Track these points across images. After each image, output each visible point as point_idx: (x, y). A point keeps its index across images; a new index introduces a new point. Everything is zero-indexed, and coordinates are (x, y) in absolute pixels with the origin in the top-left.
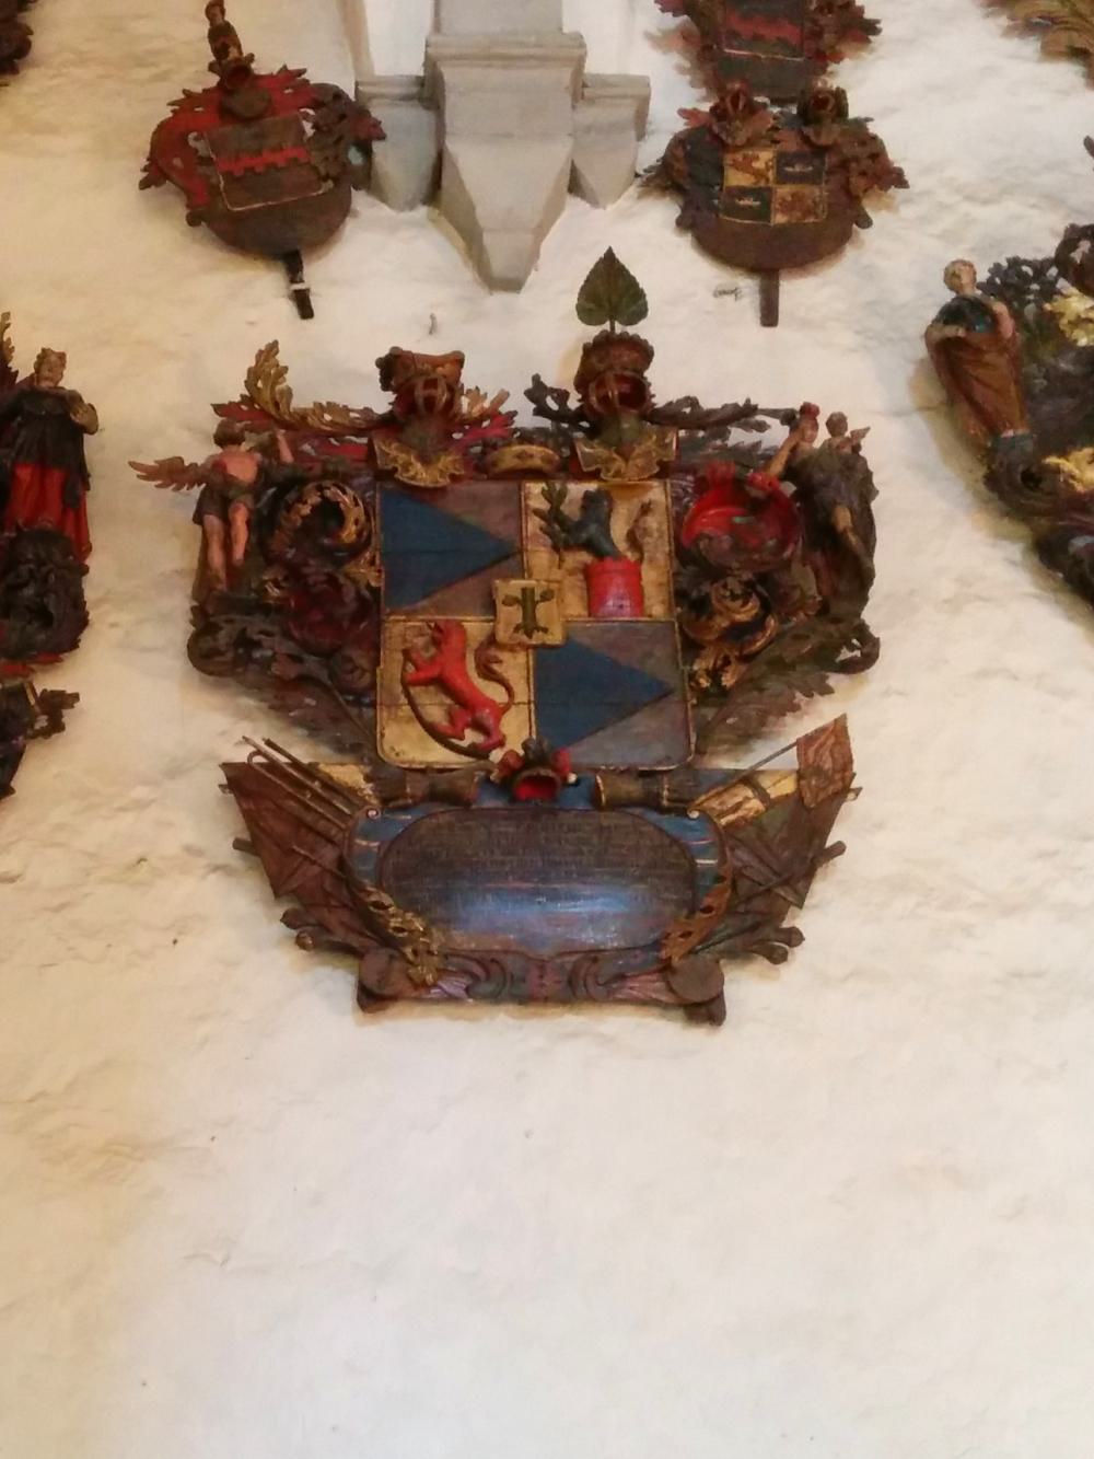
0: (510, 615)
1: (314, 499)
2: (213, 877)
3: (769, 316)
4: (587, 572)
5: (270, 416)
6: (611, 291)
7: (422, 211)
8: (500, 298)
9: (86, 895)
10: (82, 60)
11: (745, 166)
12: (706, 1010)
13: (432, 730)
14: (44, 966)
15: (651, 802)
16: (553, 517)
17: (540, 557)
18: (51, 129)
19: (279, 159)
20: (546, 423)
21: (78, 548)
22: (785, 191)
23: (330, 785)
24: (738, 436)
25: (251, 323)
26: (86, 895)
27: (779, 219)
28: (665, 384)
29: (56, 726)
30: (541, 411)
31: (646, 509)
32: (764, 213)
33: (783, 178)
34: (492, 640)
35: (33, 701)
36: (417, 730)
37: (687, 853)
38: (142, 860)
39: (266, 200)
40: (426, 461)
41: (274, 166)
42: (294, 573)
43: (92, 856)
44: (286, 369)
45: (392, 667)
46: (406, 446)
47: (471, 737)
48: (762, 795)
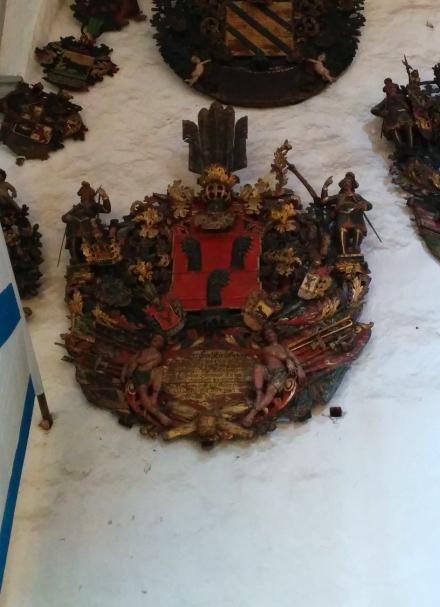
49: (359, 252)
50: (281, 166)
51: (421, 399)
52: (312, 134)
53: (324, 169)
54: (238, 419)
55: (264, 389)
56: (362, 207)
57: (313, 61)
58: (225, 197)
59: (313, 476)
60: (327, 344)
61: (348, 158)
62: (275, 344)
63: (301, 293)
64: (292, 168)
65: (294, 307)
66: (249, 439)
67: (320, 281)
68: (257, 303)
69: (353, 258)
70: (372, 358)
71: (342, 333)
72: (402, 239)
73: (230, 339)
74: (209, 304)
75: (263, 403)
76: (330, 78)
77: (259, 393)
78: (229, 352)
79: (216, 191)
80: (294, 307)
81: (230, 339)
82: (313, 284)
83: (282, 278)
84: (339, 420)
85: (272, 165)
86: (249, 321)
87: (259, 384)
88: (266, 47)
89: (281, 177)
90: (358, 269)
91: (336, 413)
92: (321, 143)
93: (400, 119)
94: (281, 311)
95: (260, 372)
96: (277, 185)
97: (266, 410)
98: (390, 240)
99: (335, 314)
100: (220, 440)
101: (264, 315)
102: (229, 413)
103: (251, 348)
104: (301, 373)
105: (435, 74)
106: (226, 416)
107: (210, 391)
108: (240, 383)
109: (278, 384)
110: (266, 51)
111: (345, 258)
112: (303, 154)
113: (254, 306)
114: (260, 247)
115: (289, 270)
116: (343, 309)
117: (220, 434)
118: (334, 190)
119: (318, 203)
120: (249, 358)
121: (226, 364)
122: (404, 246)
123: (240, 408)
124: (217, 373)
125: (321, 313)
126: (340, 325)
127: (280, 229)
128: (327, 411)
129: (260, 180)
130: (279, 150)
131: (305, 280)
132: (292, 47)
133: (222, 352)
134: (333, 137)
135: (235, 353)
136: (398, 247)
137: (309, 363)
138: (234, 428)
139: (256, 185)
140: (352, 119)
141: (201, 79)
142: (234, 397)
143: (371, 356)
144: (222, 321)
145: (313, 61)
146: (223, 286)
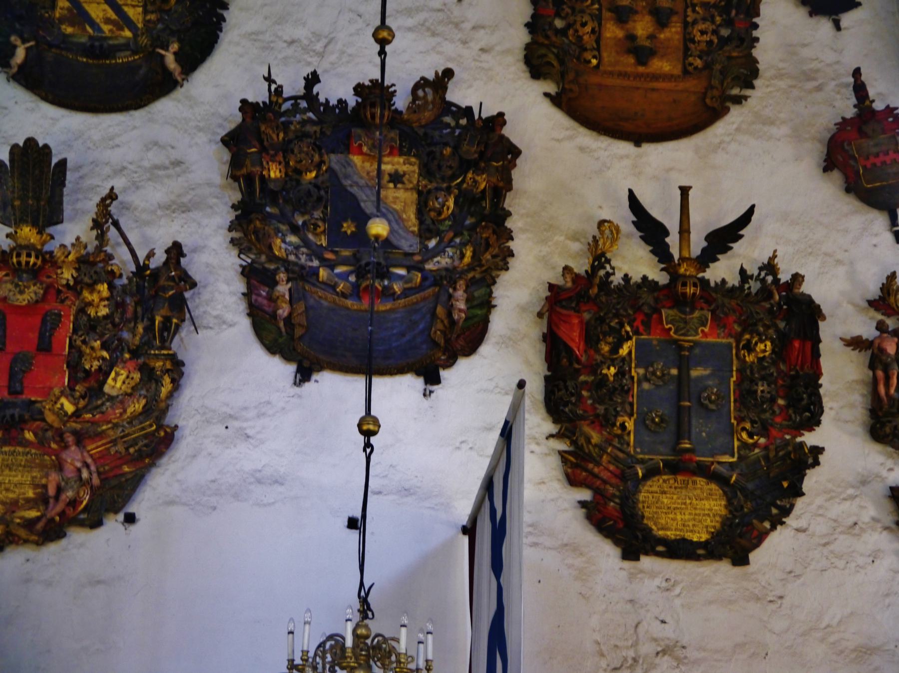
2: (885, 533)
5: (893, 309)
10: (780, 76)
18: (771, 122)
19: (888, 159)
25: (875, 246)
29: (816, 463)
35: (807, 451)
38: (856, 524)
39: (881, 182)
41: (884, 163)
43: (835, 521)
49: (170, 349)
50: (104, 218)
51: (214, 508)
52: (155, 157)
53: (159, 213)
54: (29, 524)
55: (57, 498)
56: (194, 265)
57: (163, 52)
58: (35, 264)
59: (99, 582)
60: (127, 449)
61: (189, 197)
62: (73, 448)
63: (106, 389)
64: (116, 224)
65: (99, 402)
66: (39, 544)
67: (128, 377)
68: (58, 398)
69: (164, 355)
70: (174, 462)
71: (146, 436)
72: (229, 317)
73: (29, 436)
74: (10, 393)
75: (54, 512)
76: (179, 79)
77: (52, 501)
78: (28, 450)
79: (24, 259)
80: (99, 402)
81: (29, 436)
82: (121, 378)
83: (88, 373)
84: (133, 528)
85: (93, 220)
86: (50, 418)
87: (52, 491)
88: (107, 21)
89: (102, 237)
90: (168, 365)
91: (130, 519)
92: (161, 173)
93: (248, 162)
94: (85, 407)
95: (54, 478)
96: (97, 247)
97: (57, 518)
98: (216, 317)
99: (140, 414)
100: (11, 543)
101: (66, 413)
102: (21, 518)
103: (50, 447)
104: (96, 481)
105: (305, 88)
106: (18, 521)
107: (4, 492)
108: (35, 486)
109: (70, 494)
110: (106, 28)
111: (155, 355)
112: (138, 188)
113: (56, 403)
114: (71, 326)
115: (96, 364)
116: (147, 411)
117: (11, 538)
118: (160, 258)
119: (141, 269)
120: (46, 457)
121: (23, 463)
122: (231, 326)
123: (33, 514)
124: (14, 473)
125: (125, 411)
126: (143, 429)
127: (92, 312)
128: (121, 517)
129: (78, 239)
130: (103, 200)
131: (113, 374)
132: (140, 25)
133: (20, 449)
134: (178, 163)
135: (33, 451)
136: (224, 326)
137: (107, 468)
138: (22, 533)
139: (73, 245)
140: (202, 138)
141: (21, 67)
142: (28, 500)
143: (173, 459)
144: (21, 417)
145: (163, 52)
146: (24, 372)
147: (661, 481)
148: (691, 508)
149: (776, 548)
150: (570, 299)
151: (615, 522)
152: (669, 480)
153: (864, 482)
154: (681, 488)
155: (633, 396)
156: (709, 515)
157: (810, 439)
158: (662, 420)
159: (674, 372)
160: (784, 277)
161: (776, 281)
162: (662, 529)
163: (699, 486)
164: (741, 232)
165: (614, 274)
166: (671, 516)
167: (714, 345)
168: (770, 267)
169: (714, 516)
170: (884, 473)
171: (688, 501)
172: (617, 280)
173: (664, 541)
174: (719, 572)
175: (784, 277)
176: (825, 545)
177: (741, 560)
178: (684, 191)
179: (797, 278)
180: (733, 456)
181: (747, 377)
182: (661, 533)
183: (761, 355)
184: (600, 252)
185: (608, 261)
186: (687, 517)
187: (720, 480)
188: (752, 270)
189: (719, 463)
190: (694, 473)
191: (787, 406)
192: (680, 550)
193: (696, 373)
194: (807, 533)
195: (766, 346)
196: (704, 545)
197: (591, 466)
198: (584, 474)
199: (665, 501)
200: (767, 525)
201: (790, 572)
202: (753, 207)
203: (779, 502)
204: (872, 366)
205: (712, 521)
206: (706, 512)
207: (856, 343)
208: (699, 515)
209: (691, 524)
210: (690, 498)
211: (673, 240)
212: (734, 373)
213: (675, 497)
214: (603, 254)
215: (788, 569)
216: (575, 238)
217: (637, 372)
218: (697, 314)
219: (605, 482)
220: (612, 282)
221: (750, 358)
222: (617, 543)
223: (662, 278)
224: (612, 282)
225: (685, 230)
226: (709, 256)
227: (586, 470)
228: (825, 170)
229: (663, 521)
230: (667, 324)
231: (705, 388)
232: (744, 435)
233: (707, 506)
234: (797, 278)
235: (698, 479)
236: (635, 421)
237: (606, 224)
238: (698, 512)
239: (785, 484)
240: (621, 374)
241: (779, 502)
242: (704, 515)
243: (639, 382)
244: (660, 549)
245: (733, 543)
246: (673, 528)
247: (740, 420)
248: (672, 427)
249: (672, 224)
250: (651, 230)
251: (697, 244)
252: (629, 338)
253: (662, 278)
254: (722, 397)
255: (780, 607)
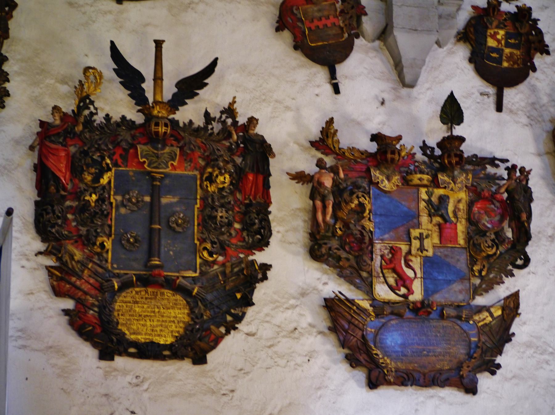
0: (416, 244)
1: (356, 202)
2: (319, 337)
3: (499, 108)
4: (439, 225)
5: (331, 149)
6: (452, 112)
7: (377, 43)
8: (405, 91)
9: (279, 342)
11: (494, 36)
12: (471, 389)
13: (390, 287)
14: (267, 368)
15: (459, 318)
16: (429, 202)
17: (424, 219)
20: (426, 159)
21: (268, 202)
22: (507, 51)
23: (359, 307)
24: (490, 170)
25: (317, 95)
26: (279, 342)
27: (505, 64)
28: (467, 149)
29: (265, 278)
30: (425, 154)
31: (459, 201)
32: (499, 61)
33: (508, 45)
34: (409, 253)
35: (257, 268)
36: (386, 287)
37: (468, 336)
38: (296, 329)
39: (323, 42)
40: (389, 179)
42: (346, 225)
43: (279, 326)
44: (337, 130)
45: (377, 261)
46: (382, 173)
47: (403, 291)
48: (491, 315)
147: (134, 292)
148: (159, 317)
149: (230, 350)
150: (58, 134)
151: (93, 327)
152: (140, 291)
153: (303, 294)
154: (151, 299)
155: (111, 220)
156: (174, 322)
157: (260, 257)
158: (136, 241)
159: (147, 199)
160: (242, 120)
161: (235, 123)
162: (134, 333)
163: (166, 297)
164: (206, 81)
165: (96, 114)
166: (142, 322)
167: (181, 176)
168: (230, 111)
169: (178, 322)
170: (320, 287)
171: (157, 310)
172: (99, 118)
173: (135, 344)
174: (183, 369)
175: (242, 120)
176: (270, 347)
177: (200, 359)
178: (159, 44)
179: (252, 121)
180: (196, 272)
181: (209, 205)
182: (133, 337)
183: (221, 186)
184: (85, 94)
185: (92, 103)
186: (155, 323)
187: (185, 292)
188: (215, 113)
189: (184, 277)
190: (162, 286)
191: (243, 229)
192: (149, 351)
193: (164, 200)
194: (256, 336)
195: (225, 178)
196: (169, 347)
197: (74, 279)
198: (68, 286)
199: (137, 309)
200: (223, 330)
201: (241, 370)
202: (217, 59)
203: (233, 311)
204: (312, 197)
205: (176, 327)
206: (172, 319)
207: (300, 177)
208: (166, 321)
209: (158, 329)
210: (158, 308)
211: (148, 86)
212: (198, 201)
213: (145, 306)
214: (88, 97)
215: (239, 367)
216: (64, 81)
217: (115, 199)
218: (167, 150)
219: (86, 293)
220: (95, 121)
221: (212, 189)
222: (95, 345)
223: (139, 119)
224: (95, 121)
225: (158, 78)
226: (177, 101)
227: (69, 283)
228: (278, 29)
229: (135, 327)
230: (141, 159)
231: (173, 214)
232: (205, 254)
233: (173, 314)
234: (252, 121)
235: (166, 291)
236: (113, 240)
237: (91, 70)
238: (164, 319)
239: (239, 296)
240: (101, 200)
241: (233, 311)
242: (170, 322)
243: (117, 207)
244: (132, 350)
245: (194, 346)
246: (143, 333)
247: (203, 241)
248: (145, 246)
249: (148, 72)
250: (129, 77)
251: (169, 90)
252: (109, 169)
253: (139, 119)
254: (188, 221)
255: (231, 399)
